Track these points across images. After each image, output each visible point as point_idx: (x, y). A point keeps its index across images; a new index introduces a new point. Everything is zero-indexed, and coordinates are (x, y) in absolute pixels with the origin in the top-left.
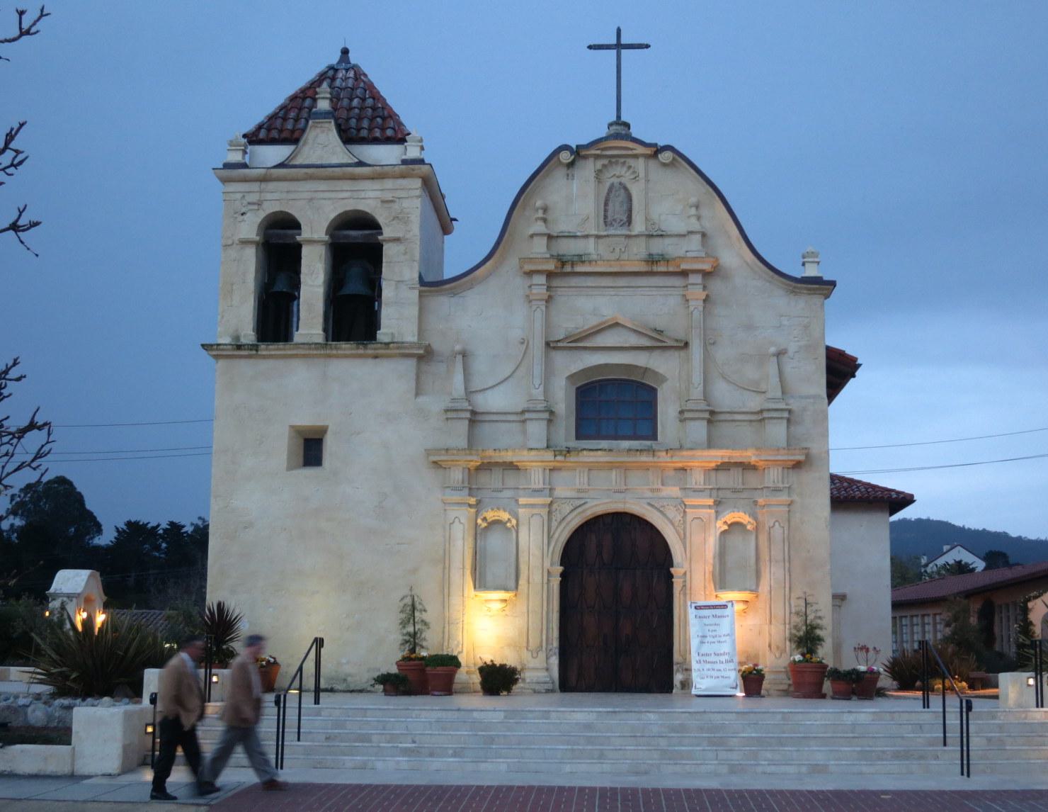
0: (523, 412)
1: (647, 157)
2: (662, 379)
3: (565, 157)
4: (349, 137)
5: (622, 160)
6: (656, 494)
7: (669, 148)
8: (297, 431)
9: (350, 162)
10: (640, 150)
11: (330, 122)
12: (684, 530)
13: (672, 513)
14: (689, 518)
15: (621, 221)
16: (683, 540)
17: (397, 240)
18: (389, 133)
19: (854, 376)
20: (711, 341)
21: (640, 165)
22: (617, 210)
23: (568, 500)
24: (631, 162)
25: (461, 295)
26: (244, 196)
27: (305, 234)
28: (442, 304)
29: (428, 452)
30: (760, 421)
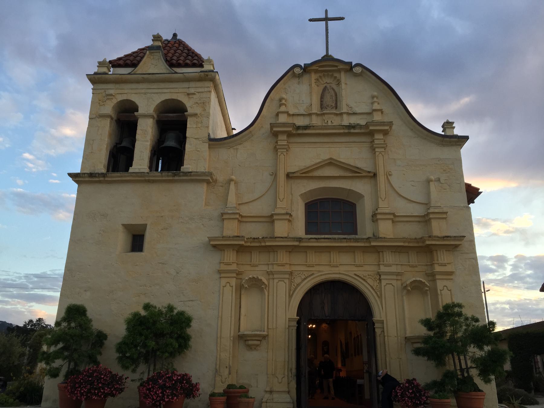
0: (272, 216)
1: (346, 71)
2: (360, 196)
3: (297, 71)
4: (171, 64)
5: (330, 74)
6: (360, 268)
7: (358, 65)
8: (127, 227)
9: (170, 72)
10: (341, 66)
11: (160, 52)
12: (381, 291)
13: (370, 281)
14: (384, 283)
15: (332, 106)
16: (380, 297)
17: (195, 115)
18: (195, 61)
19: (473, 202)
20: (390, 173)
21: (343, 77)
22: (328, 99)
23: (302, 272)
24: (336, 75)
25: (235, 147)
26: (105, 91)
27: (141, 111)
28: (224, 153)
29: (211, 239)
30: (426, 221)
